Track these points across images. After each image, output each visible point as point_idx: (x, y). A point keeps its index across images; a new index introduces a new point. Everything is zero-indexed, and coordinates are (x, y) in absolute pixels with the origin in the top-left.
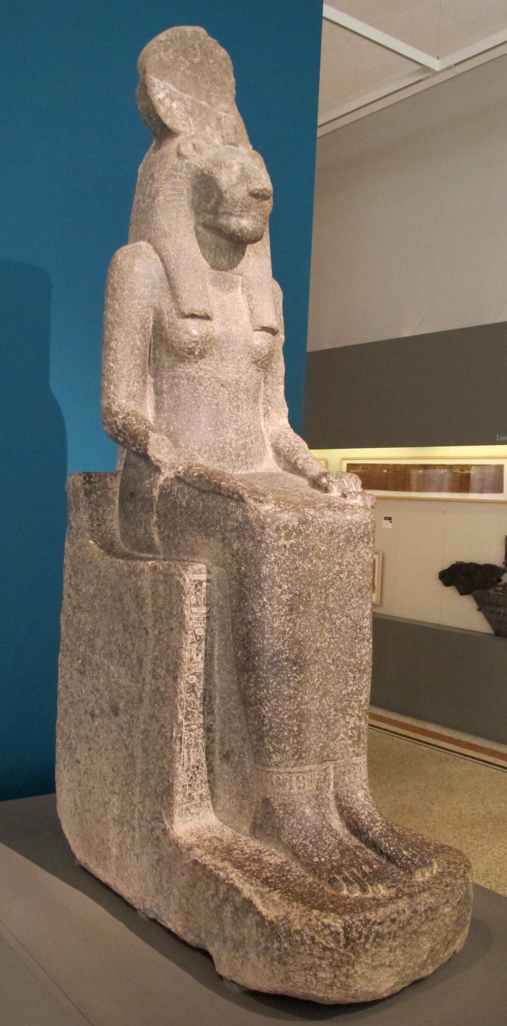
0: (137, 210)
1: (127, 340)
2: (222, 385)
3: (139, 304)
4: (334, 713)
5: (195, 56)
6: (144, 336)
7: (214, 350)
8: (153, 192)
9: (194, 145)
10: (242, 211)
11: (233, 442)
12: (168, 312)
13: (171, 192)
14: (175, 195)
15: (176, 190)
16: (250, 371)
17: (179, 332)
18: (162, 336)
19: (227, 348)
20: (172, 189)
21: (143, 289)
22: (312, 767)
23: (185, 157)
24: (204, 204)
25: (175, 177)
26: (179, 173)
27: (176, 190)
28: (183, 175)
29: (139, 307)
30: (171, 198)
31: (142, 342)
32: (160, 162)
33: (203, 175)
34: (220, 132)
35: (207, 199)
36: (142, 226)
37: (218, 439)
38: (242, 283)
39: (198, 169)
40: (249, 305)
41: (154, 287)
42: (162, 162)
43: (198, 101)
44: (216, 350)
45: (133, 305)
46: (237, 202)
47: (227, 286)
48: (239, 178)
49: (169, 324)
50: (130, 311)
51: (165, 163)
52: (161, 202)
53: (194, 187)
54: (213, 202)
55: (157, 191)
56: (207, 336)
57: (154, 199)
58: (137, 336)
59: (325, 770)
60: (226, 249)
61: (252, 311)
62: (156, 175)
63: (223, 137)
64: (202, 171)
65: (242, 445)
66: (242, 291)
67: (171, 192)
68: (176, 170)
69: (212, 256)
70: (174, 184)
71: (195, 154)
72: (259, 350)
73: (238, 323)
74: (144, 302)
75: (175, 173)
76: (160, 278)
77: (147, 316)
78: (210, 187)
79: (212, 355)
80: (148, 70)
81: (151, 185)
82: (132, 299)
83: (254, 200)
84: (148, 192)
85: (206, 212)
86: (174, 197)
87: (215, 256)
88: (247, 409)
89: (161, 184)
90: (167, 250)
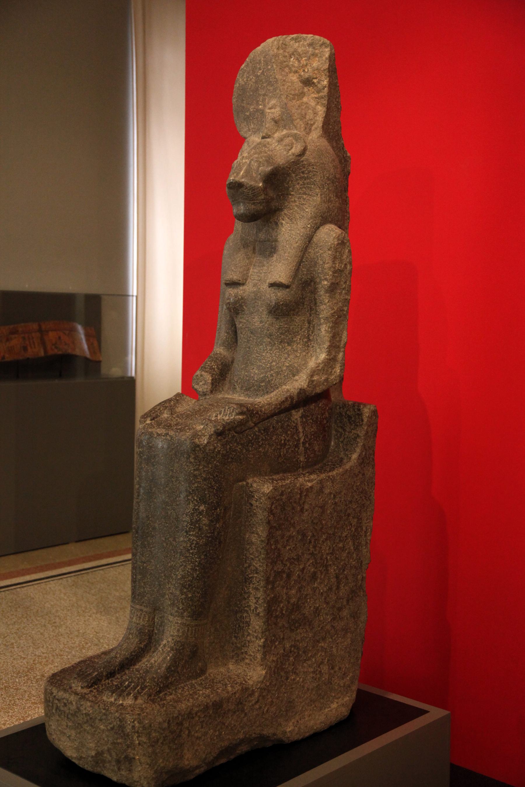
2: (252, 333)
4: (164, 577)
5: (260, 69)
7: (244, 307)
11: (256, 376)
16: (269, 319)
22: (143, 608)
37: (246, 374)
43: (257, 107)
44: (246, 307)
47: (267, 253)
59: (161, 618)
65: (262, 378)
69: (255, 232)
79: (243, 311)
87: (257, 232)
88: (271, 350)
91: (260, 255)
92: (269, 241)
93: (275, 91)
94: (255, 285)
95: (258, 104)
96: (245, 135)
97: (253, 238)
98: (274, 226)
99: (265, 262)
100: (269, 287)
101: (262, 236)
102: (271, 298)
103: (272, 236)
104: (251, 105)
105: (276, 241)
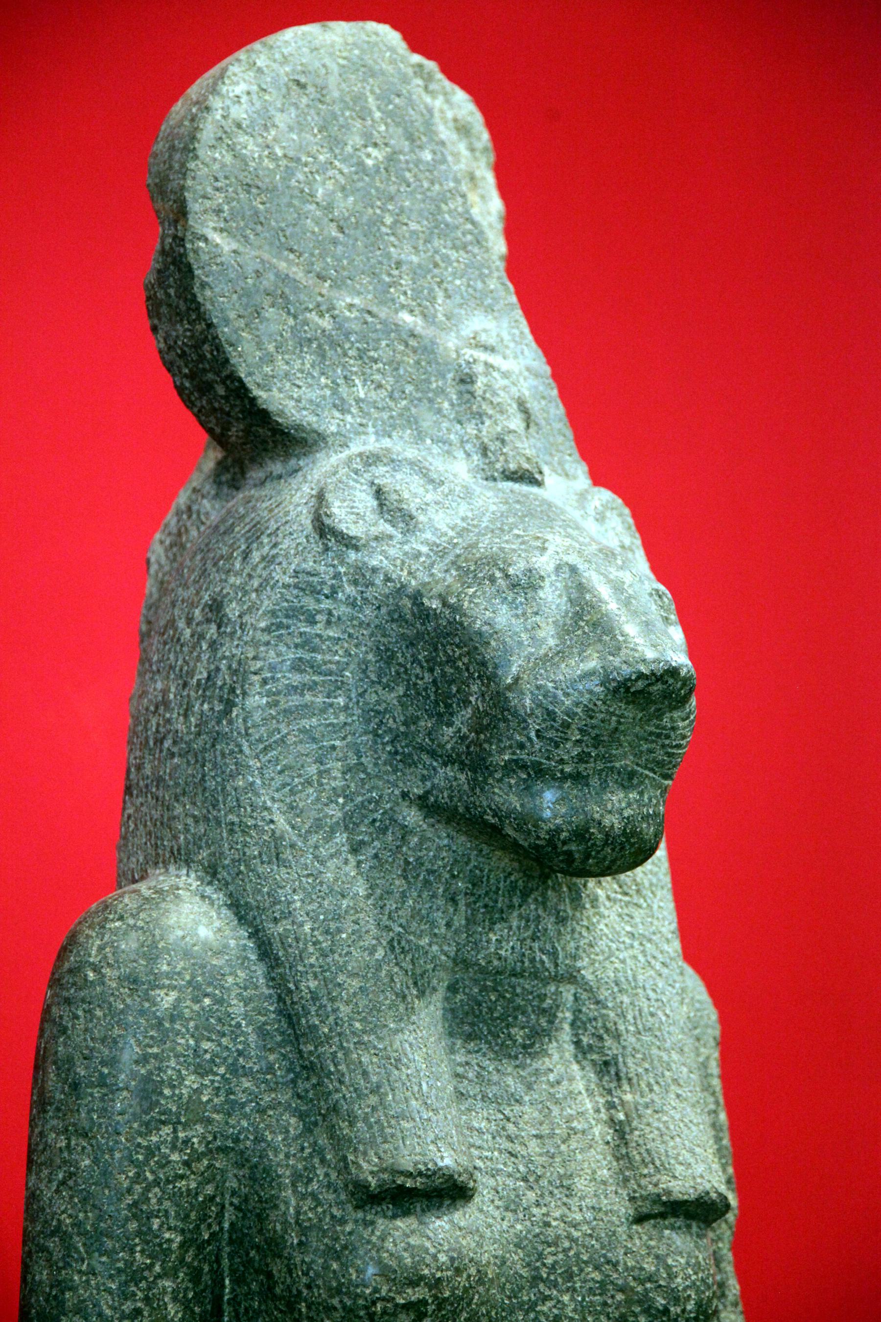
0: (159, 741)
1: (128, 1306)
3: (174, 1148)
6: (195, 1276)
8: (224, 678)
9: (379, 493)
10: (583, 758)
12: (297, 1177)
13: (296, 679)
14: (312, 687)
15: (315, 668)
17: (344, 1266)
18: (270, 1275)
19: (532, 1306)
20: (298, 666)
21: (191, 1081)
23: (349, 542)
24: (426, 723)
25: (312, 622)
26: (326, 604)
27: (315, 668)
28: (343, 610)
29: (175, 1157)
30: (295, 700)
31: (186, 1305)
32: (246, 555)
33: (425, 614)
34: (471, 429)
35: (442, 707)
36: (178, 810)
38: (577, 1012)
39: (401, 590)
40: (610, 1106)
41: (234, 1069)
42: (256, 556)
43: (384, 313)
45: (150, 1152)
46: (566, 726)
47: (519, 1034)
48: (564, 631)
49: (304, 1231)
50: (139, 1177)
51: (269, 560)
52: (257, 717)
53: (386, 656)
54: (463, 718)
55: (240, 672)
56: (458, 1271)
57: (230, 704)
58: (168, 1284)
60: (513, 887)
61: (621, 1131)
62: (232, 610)
63: (484, 451)
64: (416, 598)
66: (578, 1044)
67: (296, 679)
68: (315, 592)
69: (459, 921)
70: (306, 643)
71: (385, 527)
72: (661, 1301)
73: (569, 1191)
74: (196, 1134)
75: (309, 602)
76: (261, 1032)
77: (209, 1190)
78: (451, 661)
80: (195, 207)
81: (213, 645)
82: (149, 1128)
83: (630, 713)
84: (202, 674)
85: (433, 754)
86: (308, 697)
87: (470, 921)
89: (255, 644)
90: (288, 915)
91: (469, 1037)
92: (535, 975)
93: (482, 277)
94: (512, 1206)
95: (383, 296)
96: (308, 419)
97: (452, 950)
98: (567, 907)
99: (510, 1081)
100: (640, 1219)
101: (502, 943)
102: (671, 1276)
103: (554, 955)
104: (337, 285)
105: (572, 977)
